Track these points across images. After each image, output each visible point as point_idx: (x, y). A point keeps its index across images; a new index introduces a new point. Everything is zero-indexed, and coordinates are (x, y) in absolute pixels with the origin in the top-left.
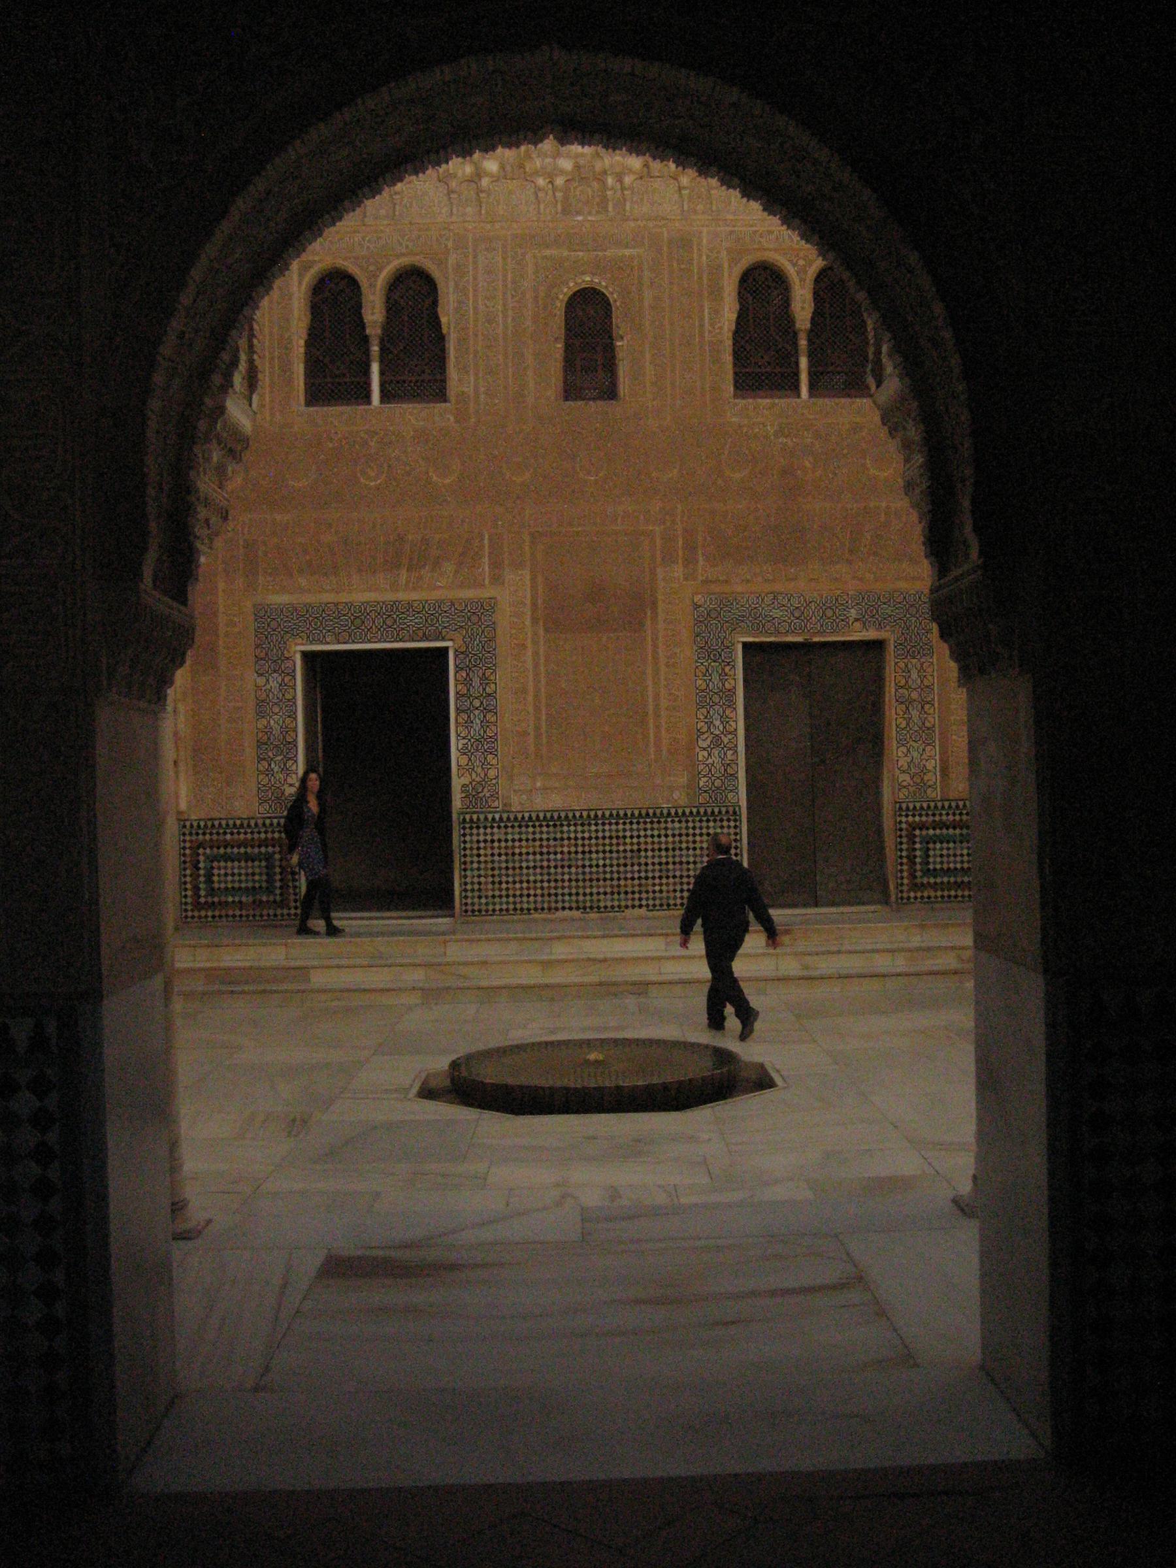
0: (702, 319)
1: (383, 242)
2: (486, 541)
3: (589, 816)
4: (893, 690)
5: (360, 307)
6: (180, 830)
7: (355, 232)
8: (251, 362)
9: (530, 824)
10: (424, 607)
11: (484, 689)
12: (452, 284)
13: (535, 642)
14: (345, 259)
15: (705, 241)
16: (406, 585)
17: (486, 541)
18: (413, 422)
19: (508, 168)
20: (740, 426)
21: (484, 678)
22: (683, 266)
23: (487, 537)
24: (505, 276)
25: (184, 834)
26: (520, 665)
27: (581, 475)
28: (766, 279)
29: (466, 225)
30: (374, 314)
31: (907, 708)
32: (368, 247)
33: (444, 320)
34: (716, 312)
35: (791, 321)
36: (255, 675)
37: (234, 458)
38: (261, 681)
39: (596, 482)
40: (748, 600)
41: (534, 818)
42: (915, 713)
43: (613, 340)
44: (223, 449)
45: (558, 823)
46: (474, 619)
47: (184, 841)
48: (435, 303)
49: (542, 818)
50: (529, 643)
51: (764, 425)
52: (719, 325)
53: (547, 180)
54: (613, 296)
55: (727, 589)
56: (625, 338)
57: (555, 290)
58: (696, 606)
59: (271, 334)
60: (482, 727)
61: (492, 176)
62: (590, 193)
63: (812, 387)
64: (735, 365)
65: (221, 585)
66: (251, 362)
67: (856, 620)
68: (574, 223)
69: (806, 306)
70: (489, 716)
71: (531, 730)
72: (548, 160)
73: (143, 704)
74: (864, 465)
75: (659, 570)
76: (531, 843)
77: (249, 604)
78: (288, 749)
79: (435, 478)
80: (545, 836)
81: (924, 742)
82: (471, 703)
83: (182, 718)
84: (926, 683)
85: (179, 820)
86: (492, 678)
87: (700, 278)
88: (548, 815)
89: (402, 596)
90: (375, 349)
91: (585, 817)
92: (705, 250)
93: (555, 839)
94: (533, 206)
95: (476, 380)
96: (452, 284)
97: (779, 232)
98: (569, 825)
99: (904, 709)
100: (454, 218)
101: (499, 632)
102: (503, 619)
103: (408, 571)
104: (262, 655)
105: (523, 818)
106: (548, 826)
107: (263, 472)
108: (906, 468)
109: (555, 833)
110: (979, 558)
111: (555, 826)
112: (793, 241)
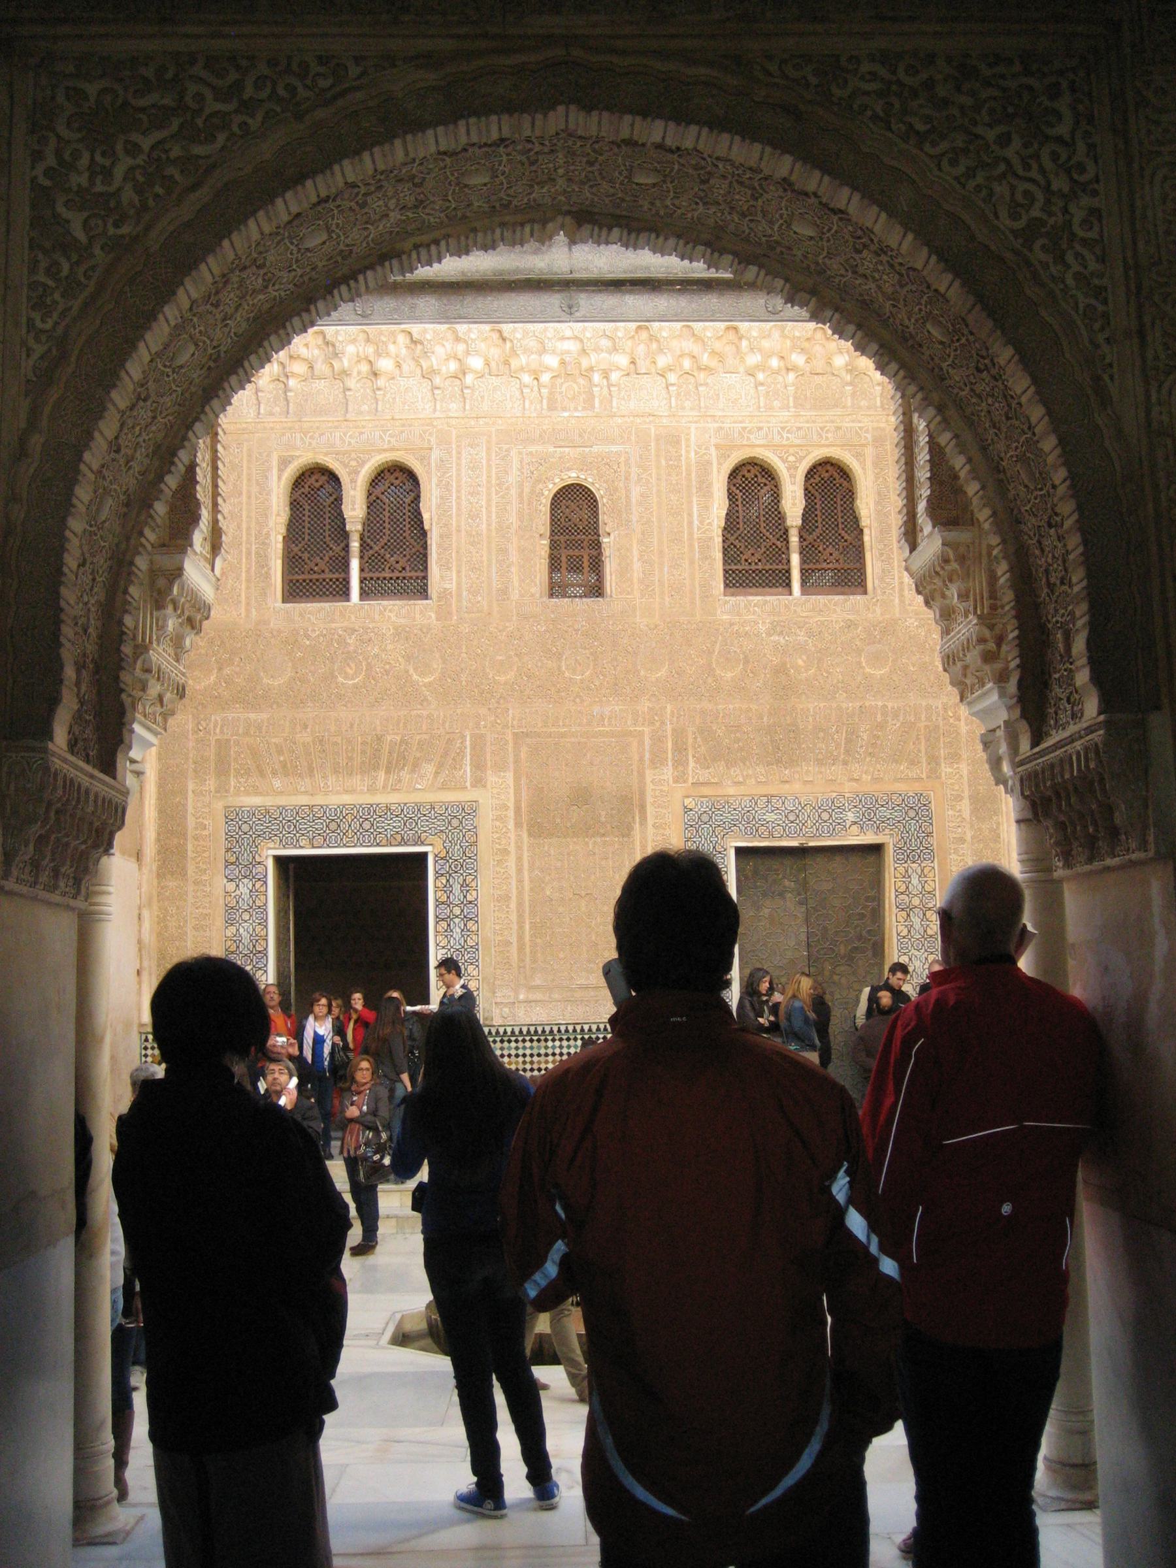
0: (690, 515)
1: (365, 437)
2: (468, 743)
3: (575, 1030)
4: (893, 896)
6: (141, 1044)
7: (336, 427)
8: (215, 522)
9: (513, 1039)
10: (402, 810)
11: (465, 897)
12: (434, 480)
13: (519, 848)
14: (326, 454)
15: (693, 438)
16: (383, 787)
17: (468, 743)
18: (394, 619)
19: (493, 365)
20: (732, 624)
21: (465, 885)
22: (671, 463)
23: (468, 738)
24: (489, 472)
25: (146, 1048)
26: (503, 871)
27: (567, 674)
28: (756, 476)
29: (450, 421)
30: (354, 509)
31: (908, 915)
32: (350, 443)
33: (426, 516)
34: (706, 508)
35: (781, 517)
36: (226, 880)
37: (193, 628)
38: (231, 886)
39: (582, 681)
40: (740, 804)
41: (517, 1033)
42: (916, 921)
43: (599, 536)
44: (179, 617)
45: (542, 1038)
46: (455, 823)
47: (146, 1056)
48: (417, 498)
49: (525, 1033)
50: (512, 848)
51: (756, 623)
54: (599, 491)
55: (720, 792)
56: (612, 535)
57: (541, 486)
58: (687, 810)
59: (249, 529)
60: (463, 936)
61: (476, 372)
62: (576, 389)
63: (802, 586)
64: (725, 562)
65: (191, 786)
66: (215, 522)
67: (855, 823)
68: (559, 419)
69: (797, 501)
70: (470, 924)
71: (514, 939)
72: (533, 357)
73: (56, 898)
74: (859, 663)
75: (647, 772)
76: (513, 1059)
77: (219, 806)
78: (257, 958)
79: (415, 677)
80: (528, 1052)
81: (926, 951)
82: (451, 911)
83: (147, 925)
84: (927, 888)
85: (140, 1033)
86: (474, 884)
87: (689, 474)
88: (532, 1029)
89: (382, 799)
90: (355, 545)
91: (571, 1031)
92: (693, 447)
93: (539, 1055)
95: (459, 576)
96: (434, 480)
97: (769, 428)
98: (553, 1040)
99: (904, 914)
100: (438, 414)
101: (481, 837)
102: (486, 824)
103: (386, 773)
104: (233, 859)
105: (505, 1032)
106: (531, 1041)
107: (238, 669)
108: (945, 640)
109: (539, 1048)
110: (1100, 714)
111: (539, 1041)
112: (782, 437)
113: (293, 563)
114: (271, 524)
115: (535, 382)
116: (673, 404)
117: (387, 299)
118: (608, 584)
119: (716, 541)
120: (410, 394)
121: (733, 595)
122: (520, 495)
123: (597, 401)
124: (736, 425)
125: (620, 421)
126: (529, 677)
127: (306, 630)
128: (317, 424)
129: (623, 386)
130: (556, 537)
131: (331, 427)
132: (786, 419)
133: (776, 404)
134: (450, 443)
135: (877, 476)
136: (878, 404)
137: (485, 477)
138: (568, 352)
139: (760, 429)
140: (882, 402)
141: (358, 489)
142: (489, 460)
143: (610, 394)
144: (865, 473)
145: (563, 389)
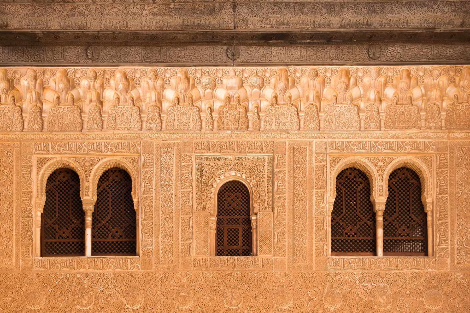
0: (311, 201)
1: (94, 146)
5: (79, 191)
7: (76, 139)
19: (181, 97)
22: (299, 166)
33: (135, 200)
52: (323, 205)
53: (207, 106)
56: (258, 214)
57: (211, 180)
68: (225, 135)
69: (383, 193)
94: (198, 124)
96: (141, 176)
97: (366, 142)
113: (48, 231)
114: (33, 203)
115: (209, 110)
116: (302, 125)
117: (109, 48)
118: (254, 247)
119: (327, 219)
120: (126, 117)
121: (337, 255)
122: (198, 187)
123: (250, 125)
124: (343, 140)
125: (265, 137)
126: (201, 308)
127: (55, 275)
128: (63, 136)
129: (268, 113)
130: (221, 217)
131: (72, 139)
132: (378, 135)
133: (372, 125)
134: (152, 151)
135: (439, 177)
136: (443, 124)
137: (174, 175)
138: (231, 88)
139: (361, 142)
140: (445, 124)
141: (91, 181)
142: (177, 163)
143: (259, 119)
144: (431, 174)
145: (228, 115)
